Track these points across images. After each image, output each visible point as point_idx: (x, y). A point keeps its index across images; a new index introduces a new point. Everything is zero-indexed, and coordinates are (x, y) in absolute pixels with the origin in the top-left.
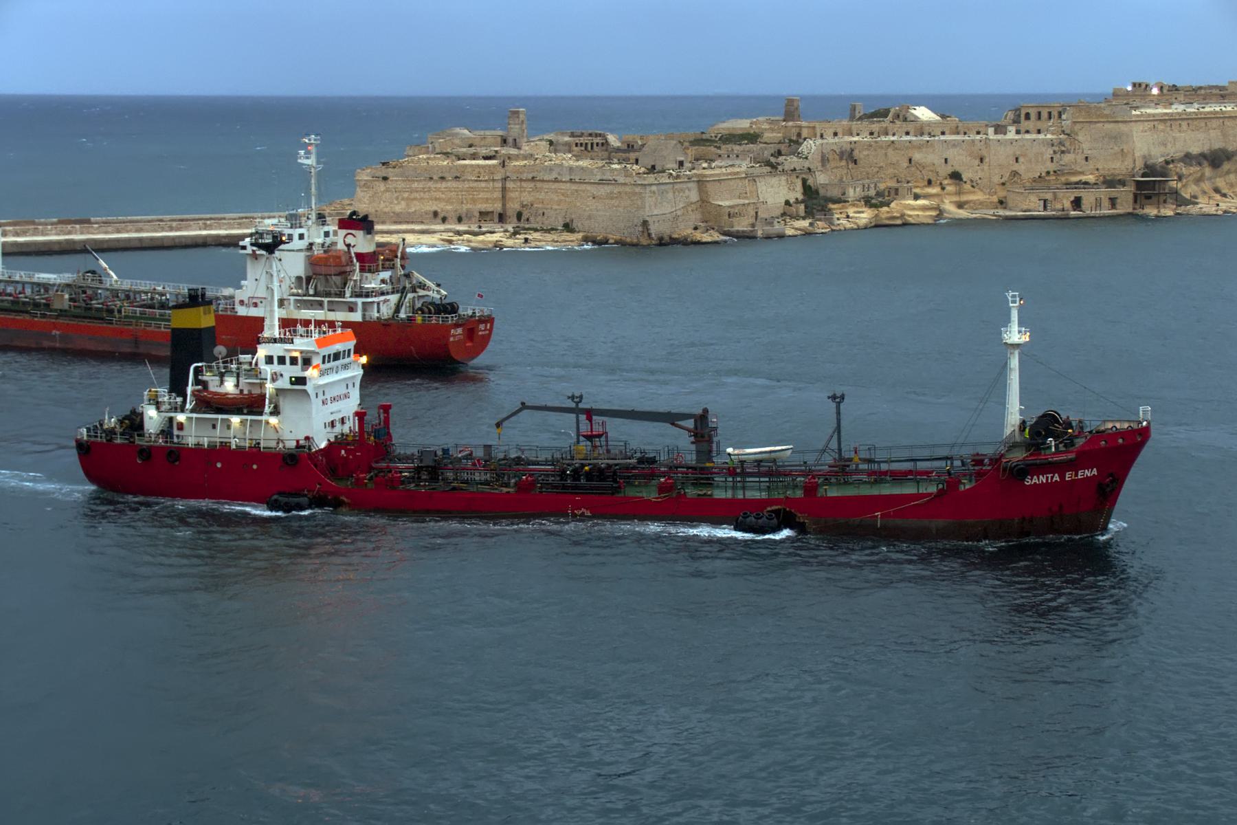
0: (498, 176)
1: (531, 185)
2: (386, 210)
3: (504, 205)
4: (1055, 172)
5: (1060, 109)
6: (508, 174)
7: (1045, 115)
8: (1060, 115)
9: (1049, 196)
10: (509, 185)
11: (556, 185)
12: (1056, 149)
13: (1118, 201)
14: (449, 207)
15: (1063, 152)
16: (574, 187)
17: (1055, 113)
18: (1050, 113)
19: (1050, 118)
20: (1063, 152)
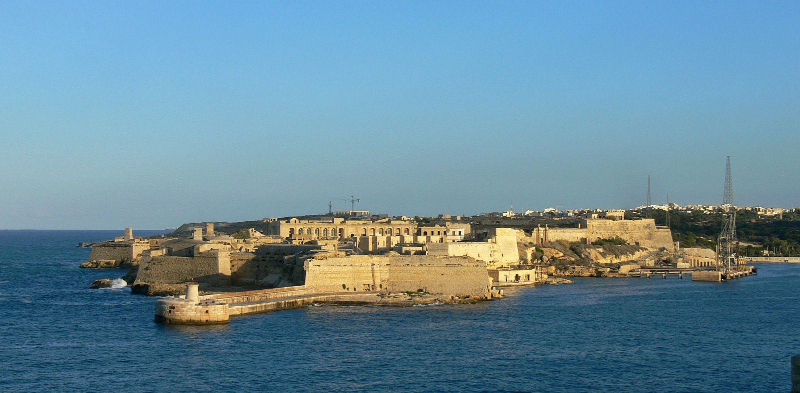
0: (370, 264)
1: (388, 268)
2: (321, 284)
3: (374, 280)
4: (493, 261)
5: (446, 230)
6: (374, 263)
7: (436, 233)
8: (445, 233)
9: (507, 274)
10: (376, 268)
11: (408, 268)
12: (491, 249)
13: (530, 276)
14: (350, 283)
15: (494, 251)
16: (425, 268)
17: (442, 232)
18: (439, 232)
19: (439, 234)
20: (494, 251)
